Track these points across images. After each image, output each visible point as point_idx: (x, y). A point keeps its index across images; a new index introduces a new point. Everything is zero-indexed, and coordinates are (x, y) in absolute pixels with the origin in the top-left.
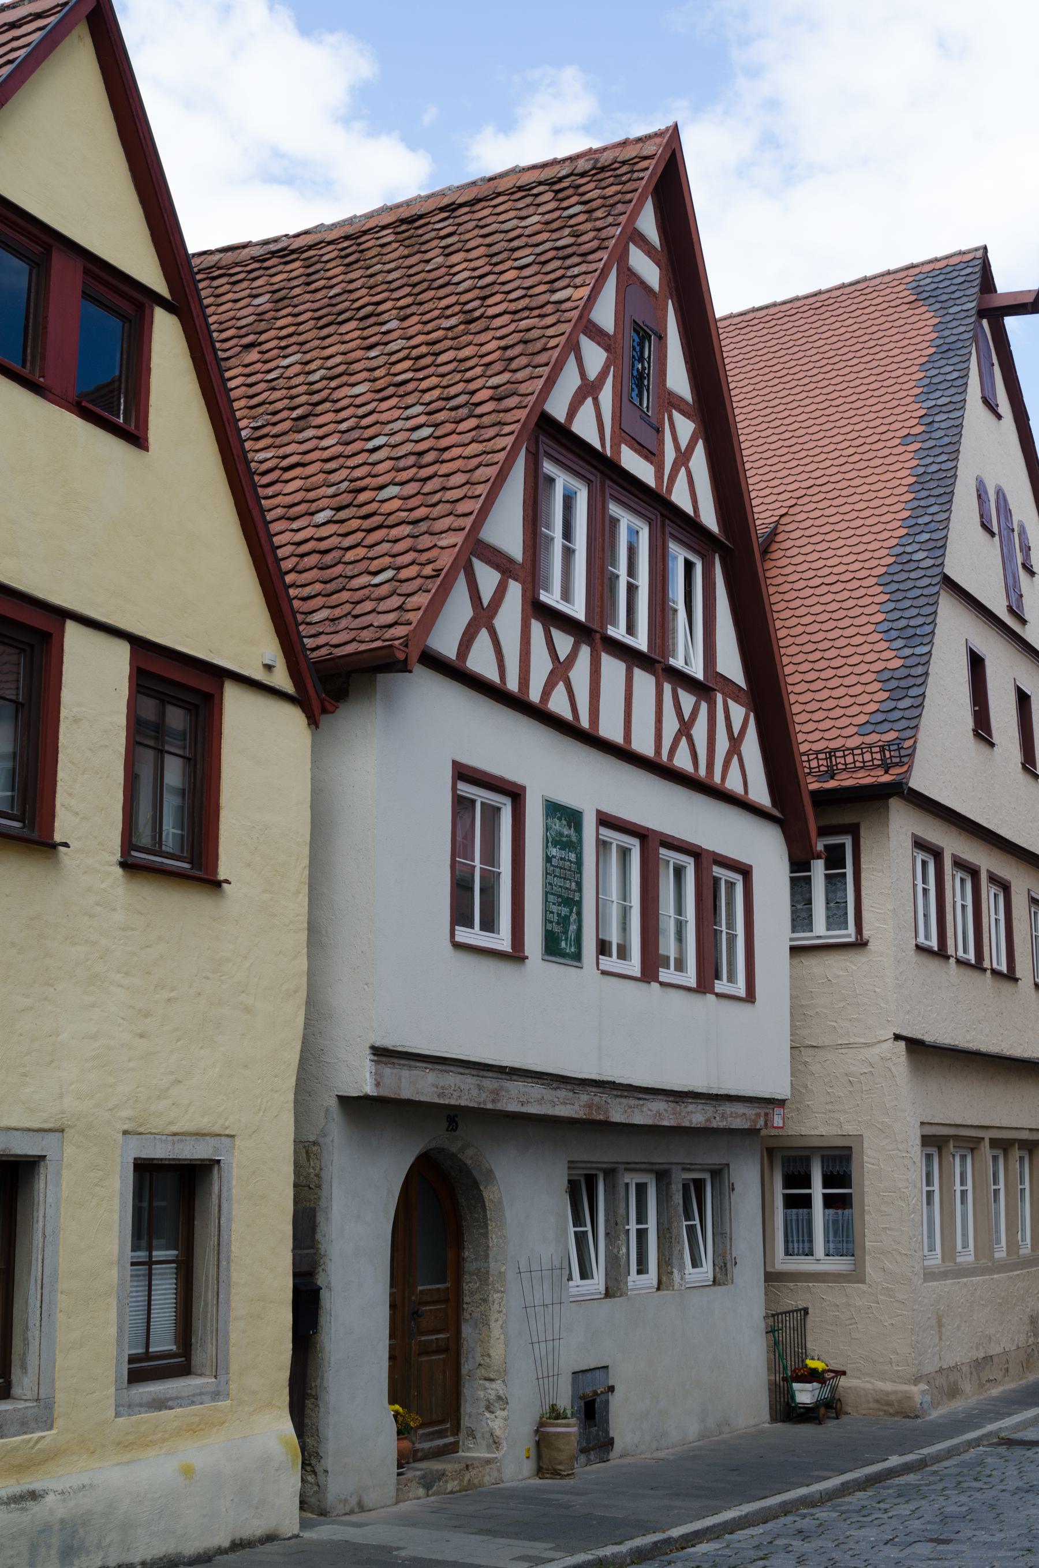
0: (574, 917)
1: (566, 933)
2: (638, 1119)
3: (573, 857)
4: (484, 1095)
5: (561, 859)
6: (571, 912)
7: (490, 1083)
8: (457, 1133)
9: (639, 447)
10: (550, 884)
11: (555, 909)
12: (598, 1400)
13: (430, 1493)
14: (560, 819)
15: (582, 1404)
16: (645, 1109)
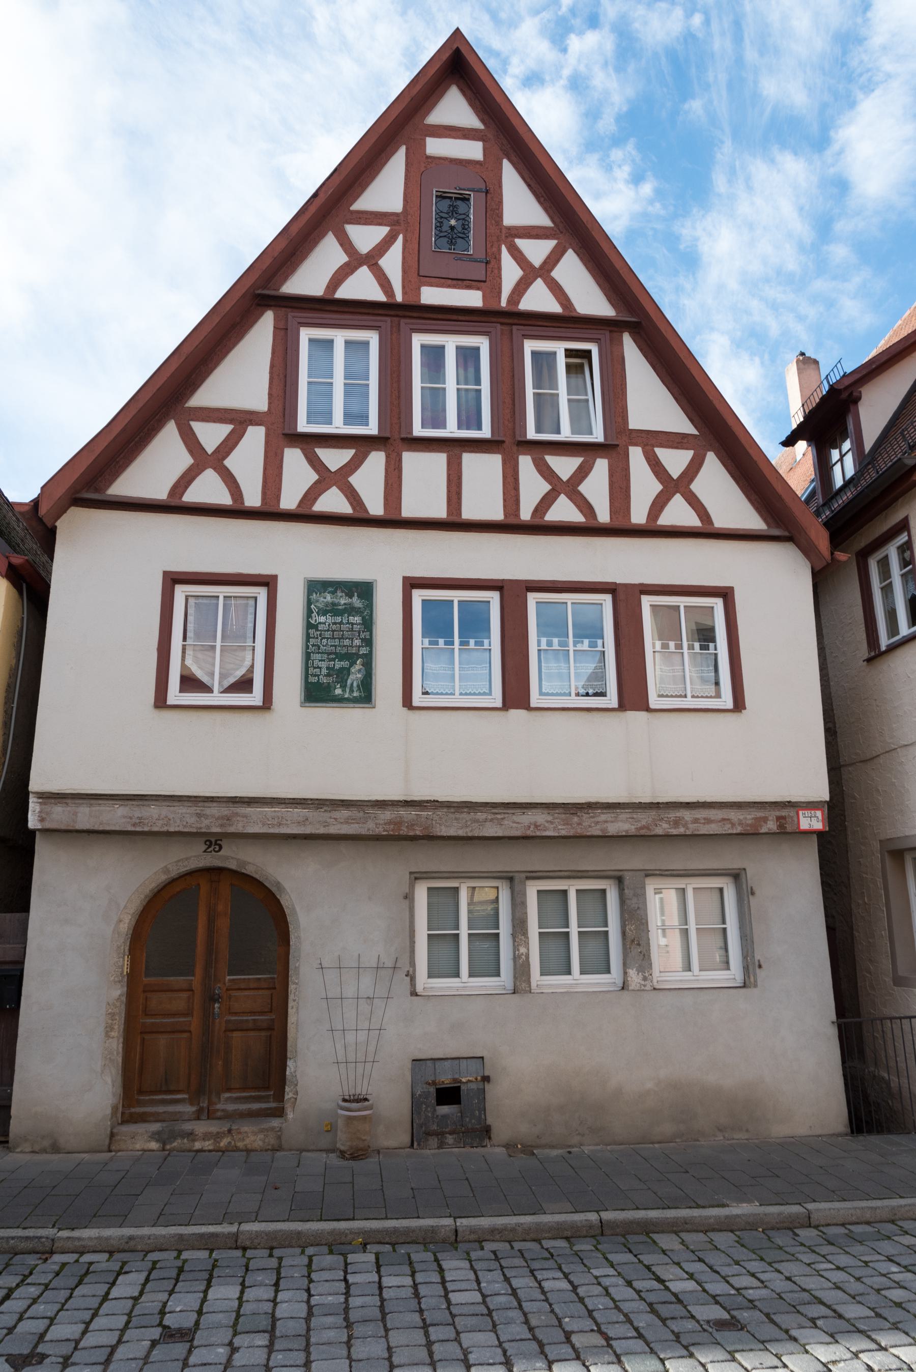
2: (491, 830)
3: (357, 619)
5: (335, 623)
6: (353, 664)
7: (214, 810)
8: (221, 853)
10: (313, 645)
11: (324, 665)
12: (463, 1087)
13: (168, 1147)
14: (333, 593)
15: (432, 1090)
16: (506, 822)
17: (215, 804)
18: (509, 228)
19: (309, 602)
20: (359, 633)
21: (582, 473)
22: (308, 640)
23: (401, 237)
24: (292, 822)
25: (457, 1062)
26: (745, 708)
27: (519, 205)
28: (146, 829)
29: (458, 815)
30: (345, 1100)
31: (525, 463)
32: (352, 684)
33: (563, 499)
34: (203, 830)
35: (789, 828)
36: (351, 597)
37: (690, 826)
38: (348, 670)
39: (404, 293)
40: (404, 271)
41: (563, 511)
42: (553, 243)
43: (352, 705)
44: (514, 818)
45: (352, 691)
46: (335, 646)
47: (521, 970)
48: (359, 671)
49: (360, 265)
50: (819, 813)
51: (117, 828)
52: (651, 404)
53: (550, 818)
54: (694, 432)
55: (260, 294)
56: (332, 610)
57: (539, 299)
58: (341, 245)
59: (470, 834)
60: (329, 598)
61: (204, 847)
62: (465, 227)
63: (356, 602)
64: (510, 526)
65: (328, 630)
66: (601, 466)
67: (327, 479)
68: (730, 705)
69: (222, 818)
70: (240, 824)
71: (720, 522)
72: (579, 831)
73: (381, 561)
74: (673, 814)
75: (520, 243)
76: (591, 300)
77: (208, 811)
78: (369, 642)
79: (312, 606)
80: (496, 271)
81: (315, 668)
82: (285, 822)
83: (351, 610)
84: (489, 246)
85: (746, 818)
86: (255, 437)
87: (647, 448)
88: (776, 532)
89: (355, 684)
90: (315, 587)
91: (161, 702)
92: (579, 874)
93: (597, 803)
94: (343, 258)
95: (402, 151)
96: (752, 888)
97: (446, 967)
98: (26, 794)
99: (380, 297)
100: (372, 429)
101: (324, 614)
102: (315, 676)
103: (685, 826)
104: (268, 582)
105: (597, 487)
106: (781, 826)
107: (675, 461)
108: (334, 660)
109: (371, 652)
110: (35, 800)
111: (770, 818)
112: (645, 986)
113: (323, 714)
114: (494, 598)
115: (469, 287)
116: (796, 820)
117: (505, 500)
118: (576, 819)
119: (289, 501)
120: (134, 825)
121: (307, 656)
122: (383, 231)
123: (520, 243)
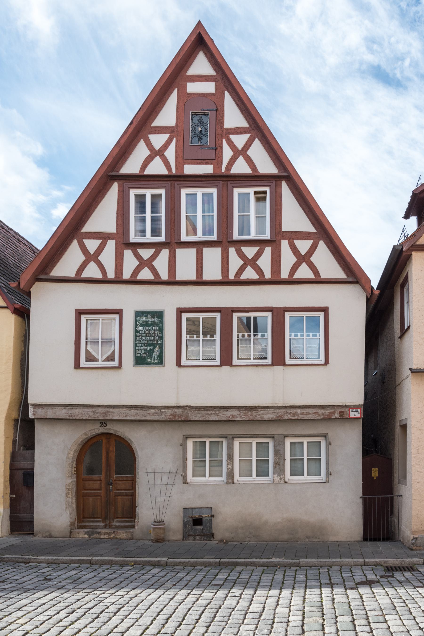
0: (157, 349)
3: (157, 328)
4: (97, 415)
5: (147, 330)
6: (155, 348)
7: (100, 410)
9: (200, 161)
10: (138, 340)
11: (143, 348)
12: (203, 519)
14: (146, 316)
15: (191, 519)
16: (220, 415)
17: (100, 408)
18: (227, 130)
19: (136, 321)
20: (157, 334)
21: (258, 255)
22: (136, 338)
23: (175, 139)
24: (131, 415)
25: (201, 509)
26: (329, 364)
27: (233, 117)
28: (74, 418)
29: (199, 412)
30: (155, 522)
31: (232, 251)
32: (155, 357)
33: (249, 268)
34: (96, 418)
35: (345, 416)
37: (300, 416)
38: (153, 350)
39: (176, 169)
40: (176, 157)
41: (249, 274)
42: (248, 136)
43: (155, 366)
44: (224, 413)
45: (154, 360)
46: (147, 340)
47: (230, 474)
48: (158, 351)
49: (156, 156)
50: (359, 410)
51: (63, 418)
52: (294, 218)
53: (239, 413)
54: (315, 231)
55: (110, 174)
56: (146, 324)
57: (241, 167)
58: (147, 146)
59: (204, 420)
60: (144, 319)
62: (206, 130)
63: (156, 320)
64: (225, 282)
65: (144, 333)
66: (268, 251)
67: (144, 263)
68: (323, 362)
69: (103, 413)
70: (111, 416)
71: (324, 275)
72: (251, 418)
73: (166, 301)
74: (292, 411)
75: (232, 137)
76: (266, 166)
77: (98, 411)
78: (162, 338)
79: (137, 323)
80: (220, 153)
81: (139, 350)
82: (128, 415)
83: (154, 324)
84: (217, 140)
86: (111, 245)
87: (291, 240)
88: (350, 279)
89: (156, 357)
90: (139, 314)
91: (77, 366)
92: (255, 436)
93: (259, 406)
94: (148, 153)
95: (176, 91)
96: (330, 442)
98: (28, 404)
99: (165, 172)
100: (162, 239)
101: (143, 326)
102: (139, 353)
103: (298, 416)
104: (119, 312)
105: (265, 262)
107: (303, 246)
108: (147, 346)
109: (162, 342)
110: (31, 407)
111: (337, 412)
112: (280, 481)
113: (143, 370)
114: (218, 316)
115: (207, 163)
116: (348, 413)
117: (222, 270)
118: (250, 413)
119: (127, 275)
120: (69, 416)
121: (136, 345)
122: (167, 136)
123: (232, 137)
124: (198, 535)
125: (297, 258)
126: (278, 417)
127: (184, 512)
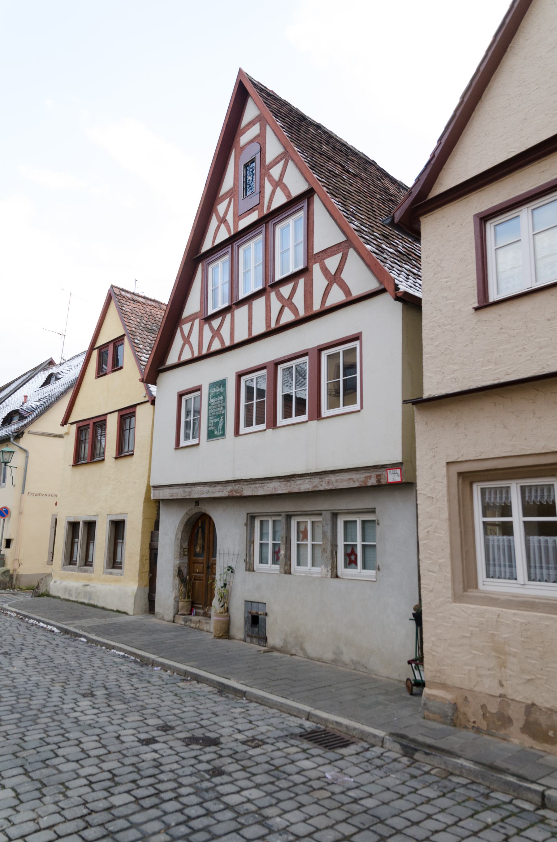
1: (217, 427)
2: (261, 492)
4: (186, 494)
7: (188, 489)
12: (260, 617)
15: (250, 615)
16: (265, 488)
35: (383, 482)
36: (220, 387)
61: (194, 504)
85: (360, 478)
91: (178, 446)
97: (263, 560)
106: (379, 481)
108: (215, 419)
111: (373, 476)
116: (386, 476)
118: (289, 484)
121: (208, 417)
124: (255, 637)
125: (328, 280)
126: (314, 487)
127: (246, 607)
